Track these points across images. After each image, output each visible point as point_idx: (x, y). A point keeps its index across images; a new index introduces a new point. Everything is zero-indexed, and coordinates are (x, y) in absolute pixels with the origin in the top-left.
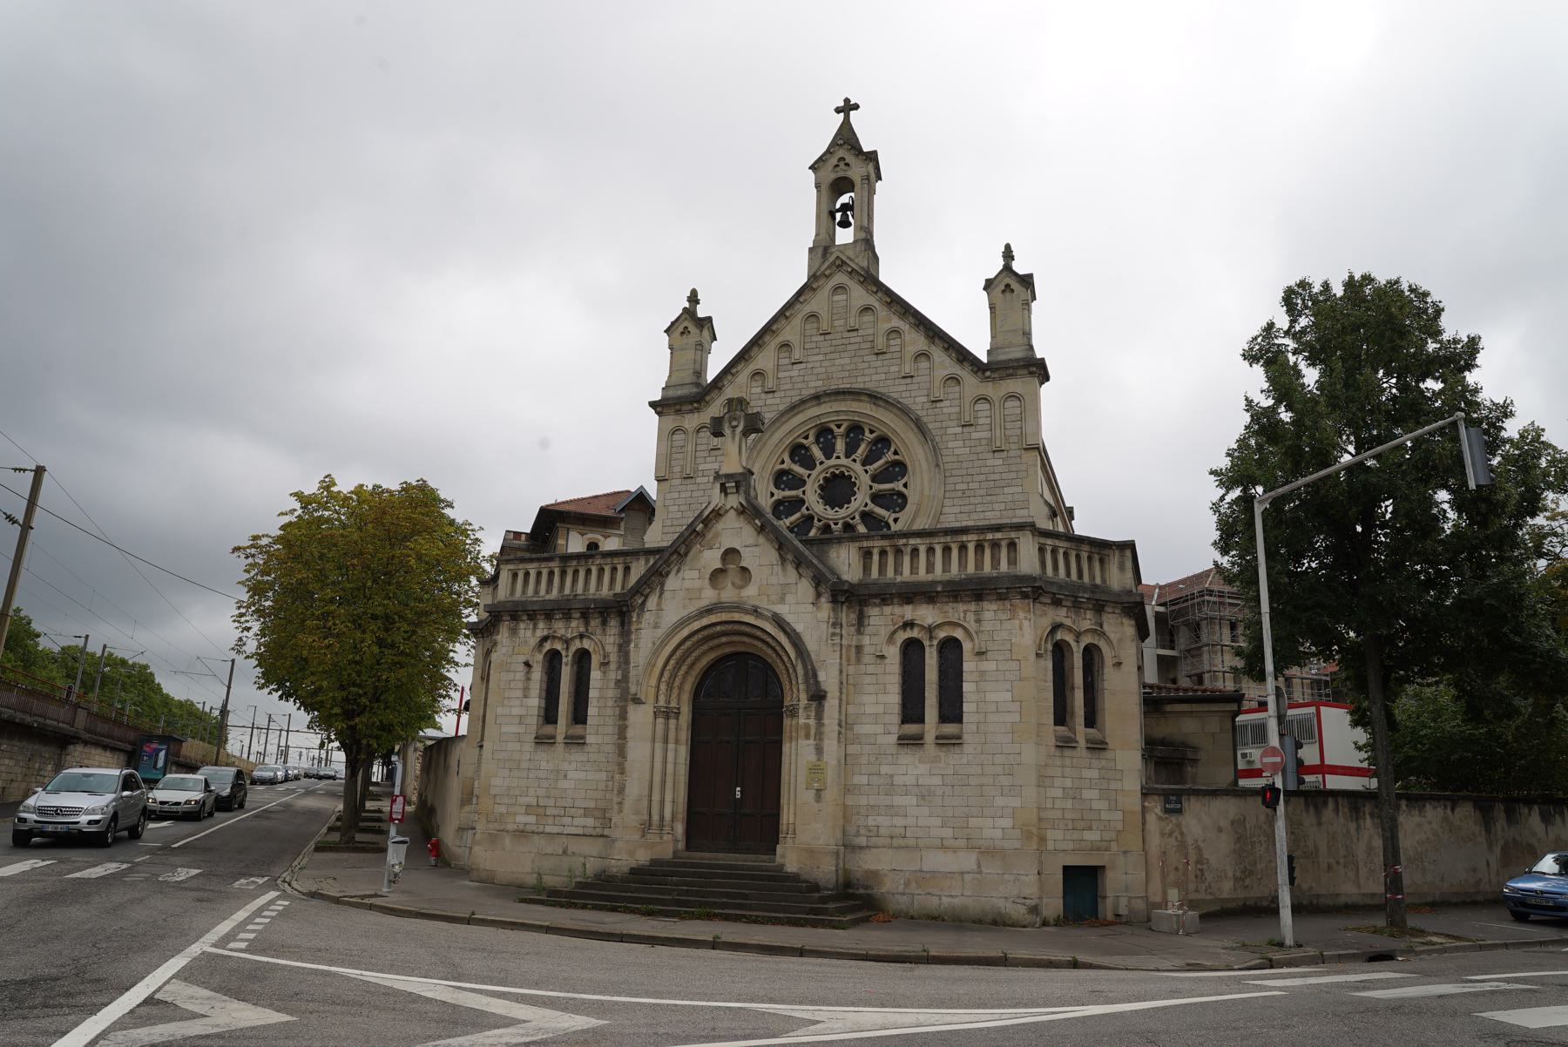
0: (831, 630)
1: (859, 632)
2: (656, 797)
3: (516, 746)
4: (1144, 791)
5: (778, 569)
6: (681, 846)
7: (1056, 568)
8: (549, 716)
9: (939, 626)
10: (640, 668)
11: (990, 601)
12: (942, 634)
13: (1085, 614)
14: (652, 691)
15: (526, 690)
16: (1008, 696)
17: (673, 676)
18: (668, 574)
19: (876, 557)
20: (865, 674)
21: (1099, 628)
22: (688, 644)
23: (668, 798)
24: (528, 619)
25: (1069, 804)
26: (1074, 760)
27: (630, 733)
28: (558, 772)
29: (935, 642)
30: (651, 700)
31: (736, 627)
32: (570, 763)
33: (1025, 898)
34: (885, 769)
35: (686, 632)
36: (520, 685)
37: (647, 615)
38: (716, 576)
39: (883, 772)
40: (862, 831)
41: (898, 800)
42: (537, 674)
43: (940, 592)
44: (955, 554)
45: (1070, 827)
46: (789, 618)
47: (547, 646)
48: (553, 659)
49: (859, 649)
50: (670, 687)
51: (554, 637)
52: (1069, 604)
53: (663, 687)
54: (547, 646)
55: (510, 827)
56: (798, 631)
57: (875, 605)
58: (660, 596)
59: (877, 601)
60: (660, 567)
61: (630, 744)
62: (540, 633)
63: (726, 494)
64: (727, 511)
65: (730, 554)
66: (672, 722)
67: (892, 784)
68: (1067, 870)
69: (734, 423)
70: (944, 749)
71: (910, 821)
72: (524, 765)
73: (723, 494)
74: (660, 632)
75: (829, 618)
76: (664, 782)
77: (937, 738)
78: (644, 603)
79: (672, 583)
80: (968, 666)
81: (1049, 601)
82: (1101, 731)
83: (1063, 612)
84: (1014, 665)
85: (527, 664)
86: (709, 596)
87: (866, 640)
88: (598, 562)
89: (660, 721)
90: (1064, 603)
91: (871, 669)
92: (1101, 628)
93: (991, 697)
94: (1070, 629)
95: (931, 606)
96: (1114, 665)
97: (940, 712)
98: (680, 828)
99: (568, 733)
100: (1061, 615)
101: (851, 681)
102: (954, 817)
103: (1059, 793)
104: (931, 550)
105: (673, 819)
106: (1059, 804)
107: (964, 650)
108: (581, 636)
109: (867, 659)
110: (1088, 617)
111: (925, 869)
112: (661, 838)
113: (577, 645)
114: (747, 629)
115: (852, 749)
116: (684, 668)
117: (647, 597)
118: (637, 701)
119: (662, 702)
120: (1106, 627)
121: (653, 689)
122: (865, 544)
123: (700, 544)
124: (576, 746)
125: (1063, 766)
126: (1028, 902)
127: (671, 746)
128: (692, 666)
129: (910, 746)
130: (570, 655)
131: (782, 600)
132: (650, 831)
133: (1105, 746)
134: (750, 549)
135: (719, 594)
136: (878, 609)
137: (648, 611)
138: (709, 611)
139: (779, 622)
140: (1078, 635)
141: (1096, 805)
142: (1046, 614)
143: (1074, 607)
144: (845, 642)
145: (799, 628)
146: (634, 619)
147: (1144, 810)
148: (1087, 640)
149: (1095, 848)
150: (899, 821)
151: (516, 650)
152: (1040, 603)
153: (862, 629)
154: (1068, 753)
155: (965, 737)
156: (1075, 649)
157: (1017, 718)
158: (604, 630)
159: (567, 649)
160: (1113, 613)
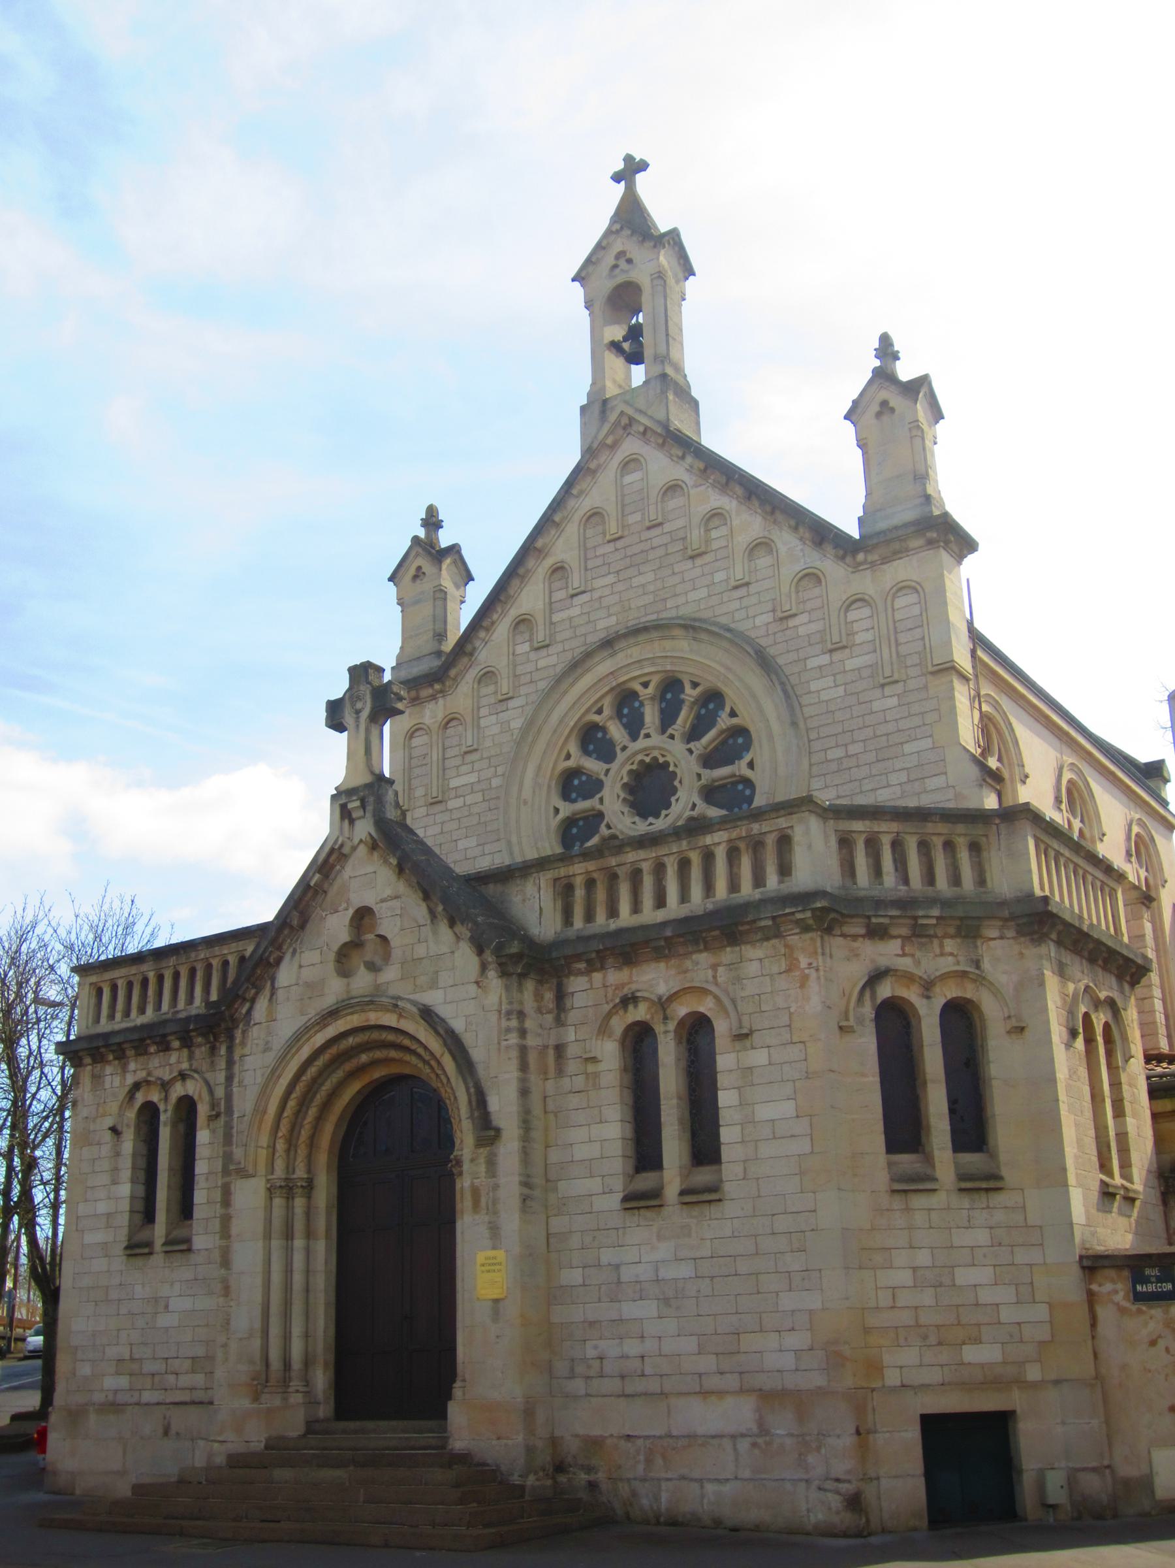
0: (504, 1023)
1: (559, 1022)
2: (275, 1330)
3: (100, 1265)
4: (1085, 1263)
5: (427, 931)
6: (324, 1411)
7: (877, 871)
8: (147, 1212)
9: (673, 997)
10: (246, 1118)
11: (752, 943)
12: (681, 1010)
13: (942, 946)
14: (263, 1154)
15: (115, 1170)
16: (788, 1108)
17: (294, 1127)
18: (279, 961)
19: (579, 893)
20: (570, 1092)
21: (972, 970)
22: (312, 1071)
23: (297, 1330)
24: (115, 1058)
25: (927, 1298)
26: (934, 1215)
27: (235, 1228)
28: (156, 1300)
29: (672, 1026)
30: (262, 1168)
31: (375, 1035)
32: (172, 1284)
33: (838, 1480)
34: (607, 1256)
35: (305, 1052)
36: (106, 1165)
37: (255, 1032)
38: (345, 956)
39: (604, 1260)
40: (580, 1369)
41: (630, 1310)
42: (128, 1144)
43: (671, 938)
44: (696, 873)
45: (933, 1340)
46: (444, 1011)
47: (140, 1098)
48: (150, 1113)
49: (560, 1049)
50: (291, 1145)
51: (148, 1083)
52: (904, 931)
53: (281, 1146)
54: (140, 1098)
55: (98, 1397)
56: (457, 1032)
57: (580, 973)
58: (272, 994)
59: (582, 966)
60: (264, 952)
61: (236, 1246)
62: (130, 1080)
63: (352, 822)
64: (354, 848)
65: (363, 916)
66: (299, 1203)
67: (619, 1282)
68: (932, 1425)
69: (359, 705)
70: (696, 1211)
71: (650, 1346)
72: (114, 1295)
73: (346, 822)
74: (270, 1058)
75: (500, 1003)
76: (287, 1303)
77: (682, 1193)
78: (249, 1011)
79: (285, 975)
80: (725, 1061)
81: (862, 931)
82: (993, 1156)
83: (894, 946)
84: (794, 1052)
85: (114, 1130)
86: (335, 989)
87: (571, 1035)
88: (202, 956)
89: (278, 1202)
90: (894, 931)
91: (579, 1082)
92: (978, 967)
93: (764, 1112)
94: (908, 978)
95: (662, 965)
96: (1009, 1032)
97: (693, 1146)
98: (321, 1379)
99: (172, 1236)
100: (887, 952)
101: (551, 1106)
102: (716, 1334)
103: (904, 1277)
104: (659, 869)
105: (307, 1362)
106: (904, 1299)
107: (717, 1034)
108: (183, 1076)
109: (572, 1067)
110: (948, 949)
111: (675, 1433)
112: (285, 1399)
113: (178, 1090)
114: (391, 1037)
115: (557, 1224)
116: (312, 1112)
117: (253, 1001)
118: (243, 1174)
119: (279, 1171)
120: (986, 965)
121: (265, 1151)
122: (563, 872)
123: (320, 906)
124: (179, 1255)
125: (910, 1228)
126: (844, 1487)
127: (299, 1243)
128: (326, 1106)
129: (642, 1211)
130: (170, 1108)
131: (433, 985)
132: (266, 1390)
133: (998, 1184)
134: (389, 903)
135: (348, 985)
136: (586, 979)
137: (255, 1024)
138: (333, 1014)
139: (427, 1014)
140: (927, 987)
141: (985, 1296)
142: (857, 955)
143: (915, 935)
144: (531, 1041)
145: (458, 1025)
146: (237, 1041)
147: (1091, 1299)
148: (948, 992)
149: (995, 1382)
150: (632, 1347)
151: (101, 1110)
152: (844, 936)
153: (562, 1016)
154: (918, 1201)
155: (727, 1187)
156: (922, 1011)
157: (804, 1146)
158: (212, 1062)
159: (166, 1099)
160: (1001, 938)
